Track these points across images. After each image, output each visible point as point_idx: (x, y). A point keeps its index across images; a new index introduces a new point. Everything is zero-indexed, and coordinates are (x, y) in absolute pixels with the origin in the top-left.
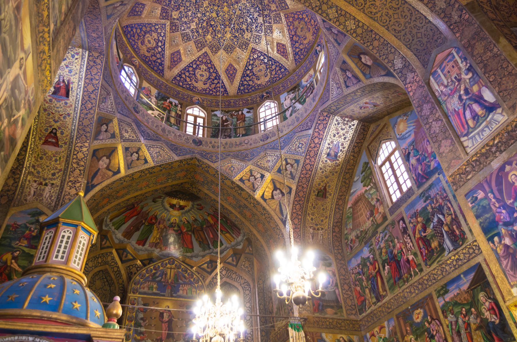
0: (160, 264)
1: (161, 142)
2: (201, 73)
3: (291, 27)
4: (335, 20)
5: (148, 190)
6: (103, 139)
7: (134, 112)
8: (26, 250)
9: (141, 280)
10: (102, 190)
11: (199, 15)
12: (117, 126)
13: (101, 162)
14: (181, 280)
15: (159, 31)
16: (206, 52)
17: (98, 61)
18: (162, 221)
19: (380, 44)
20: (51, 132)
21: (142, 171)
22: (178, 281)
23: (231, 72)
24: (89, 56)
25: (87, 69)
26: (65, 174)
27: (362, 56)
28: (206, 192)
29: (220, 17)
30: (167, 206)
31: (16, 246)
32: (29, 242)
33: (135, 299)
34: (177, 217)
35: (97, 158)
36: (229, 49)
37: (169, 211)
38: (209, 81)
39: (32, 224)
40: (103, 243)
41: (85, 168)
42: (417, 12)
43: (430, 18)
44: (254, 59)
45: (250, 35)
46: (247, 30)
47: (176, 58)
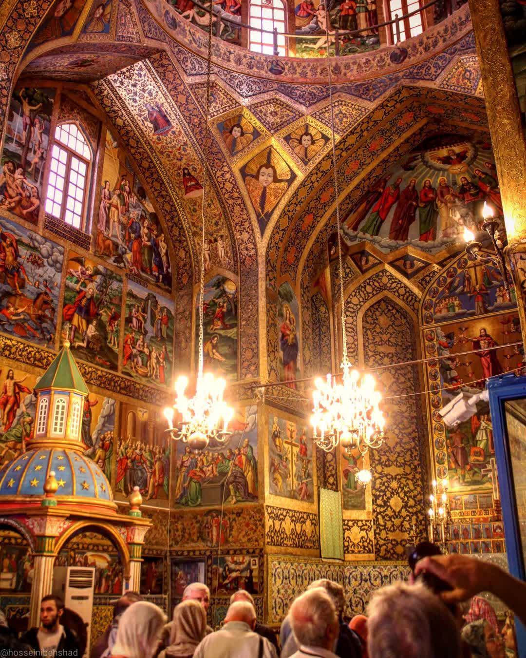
0: (455, 266)
1: (337, 95)
5: (369, 169)
6: (244, 148)
7: (273, 77)
8: (222, 332)
9: (434, 300)
10: (284, 213)
12: (254, 118)
13: (261, 178)
14: (496, 279)
17: (165, 62)
18: (445, 190)
20: (184, 174)
21: (329, 156)
22: (490, 283)
24: (152, 63)
25: (162, 80)
28: (464, 125)
30: (439, 164)
31: (212, 332)
32: (223, 323)
33: (432, 331)
34: (463, 173)
35: (252, 176)
37: (447, 170)
39: (219, 297)
40: (363, 263)
41: (242, 199)
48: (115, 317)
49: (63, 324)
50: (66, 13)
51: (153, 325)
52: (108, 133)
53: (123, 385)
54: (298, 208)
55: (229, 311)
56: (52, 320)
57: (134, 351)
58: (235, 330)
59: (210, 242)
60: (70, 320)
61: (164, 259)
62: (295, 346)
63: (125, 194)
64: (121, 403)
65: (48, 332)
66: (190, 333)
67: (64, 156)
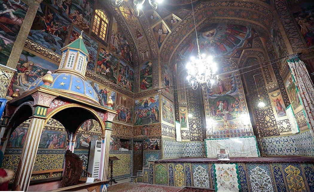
5: (188, 34)
8: (148, 76)
10: (165, 43)
13: (159, 32)
26: (149, 44)
32: (148, 74)
35: (156, 31)
48: (115, 69)
49: (97, 66)
51: (128, 74)
52: (114, 18)
53: (118, 88)
54: (169, 43)
55: (150, 70)
56: (94, 64)
57: (122, 80)
58: (152, 75)
59: (144, 53)
60: (100, 65)
61: (131, 58)
62: (168, 81)
63: (119, 36)
64: (117, 94)
65: (92, 67)
66: (139, 78)
67: (99, 19)
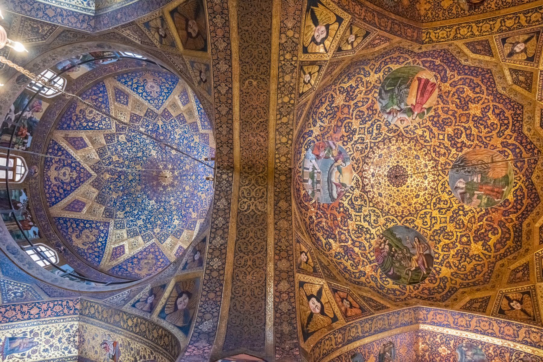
2: (67, 173)
3: (145, 253)
4: (213, 247)
11: (127, 163)
15: (104, 122)
16: (91, 175)
19: (214, 299)
23: (76, 206)
27: (184, 296)
29: (129, 184)
36: (101, 199)
38: (60, 184)
42: (263, 314)
43: (267, 329)
44: (98, 228)
45: (121, 216)
46: (126, 213)
47: (78, 144)
50: (187, 24)
